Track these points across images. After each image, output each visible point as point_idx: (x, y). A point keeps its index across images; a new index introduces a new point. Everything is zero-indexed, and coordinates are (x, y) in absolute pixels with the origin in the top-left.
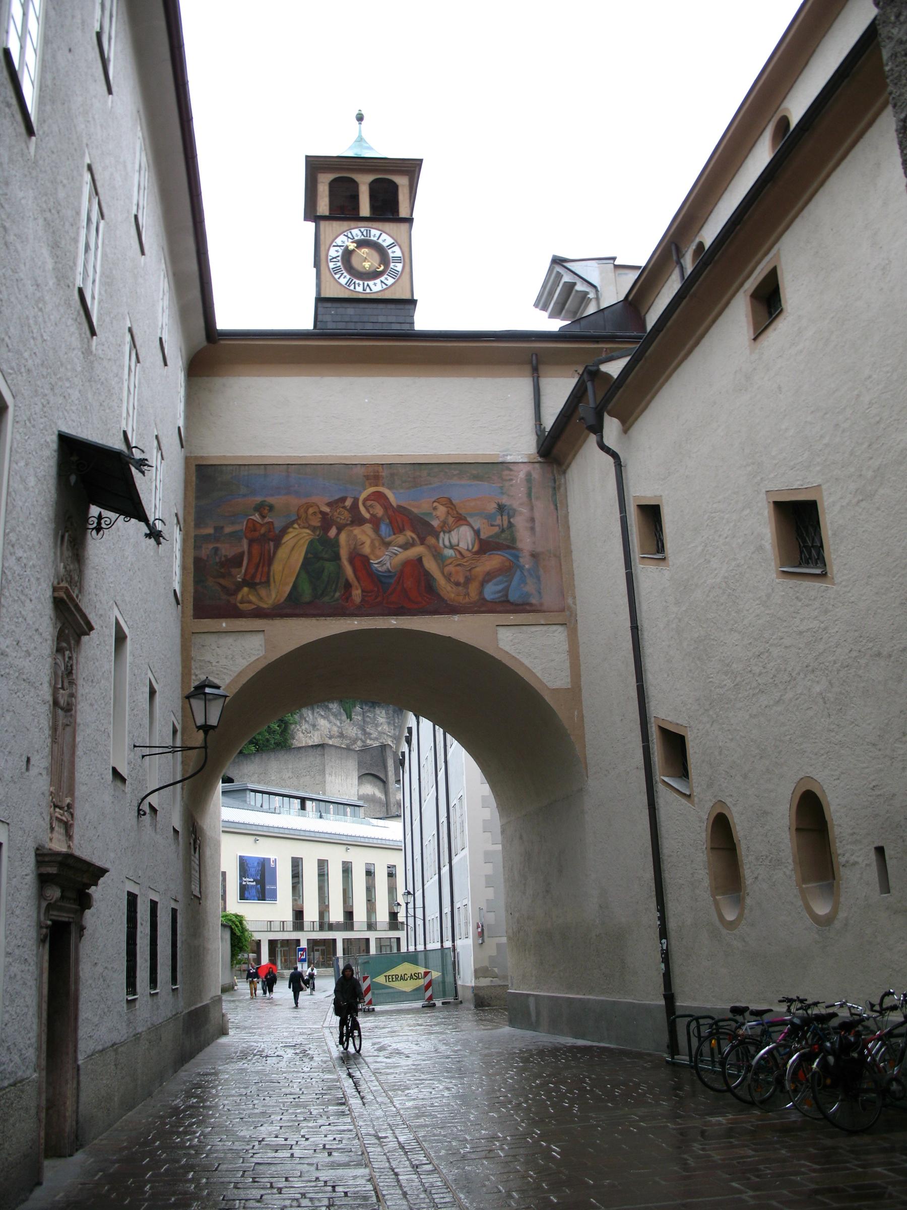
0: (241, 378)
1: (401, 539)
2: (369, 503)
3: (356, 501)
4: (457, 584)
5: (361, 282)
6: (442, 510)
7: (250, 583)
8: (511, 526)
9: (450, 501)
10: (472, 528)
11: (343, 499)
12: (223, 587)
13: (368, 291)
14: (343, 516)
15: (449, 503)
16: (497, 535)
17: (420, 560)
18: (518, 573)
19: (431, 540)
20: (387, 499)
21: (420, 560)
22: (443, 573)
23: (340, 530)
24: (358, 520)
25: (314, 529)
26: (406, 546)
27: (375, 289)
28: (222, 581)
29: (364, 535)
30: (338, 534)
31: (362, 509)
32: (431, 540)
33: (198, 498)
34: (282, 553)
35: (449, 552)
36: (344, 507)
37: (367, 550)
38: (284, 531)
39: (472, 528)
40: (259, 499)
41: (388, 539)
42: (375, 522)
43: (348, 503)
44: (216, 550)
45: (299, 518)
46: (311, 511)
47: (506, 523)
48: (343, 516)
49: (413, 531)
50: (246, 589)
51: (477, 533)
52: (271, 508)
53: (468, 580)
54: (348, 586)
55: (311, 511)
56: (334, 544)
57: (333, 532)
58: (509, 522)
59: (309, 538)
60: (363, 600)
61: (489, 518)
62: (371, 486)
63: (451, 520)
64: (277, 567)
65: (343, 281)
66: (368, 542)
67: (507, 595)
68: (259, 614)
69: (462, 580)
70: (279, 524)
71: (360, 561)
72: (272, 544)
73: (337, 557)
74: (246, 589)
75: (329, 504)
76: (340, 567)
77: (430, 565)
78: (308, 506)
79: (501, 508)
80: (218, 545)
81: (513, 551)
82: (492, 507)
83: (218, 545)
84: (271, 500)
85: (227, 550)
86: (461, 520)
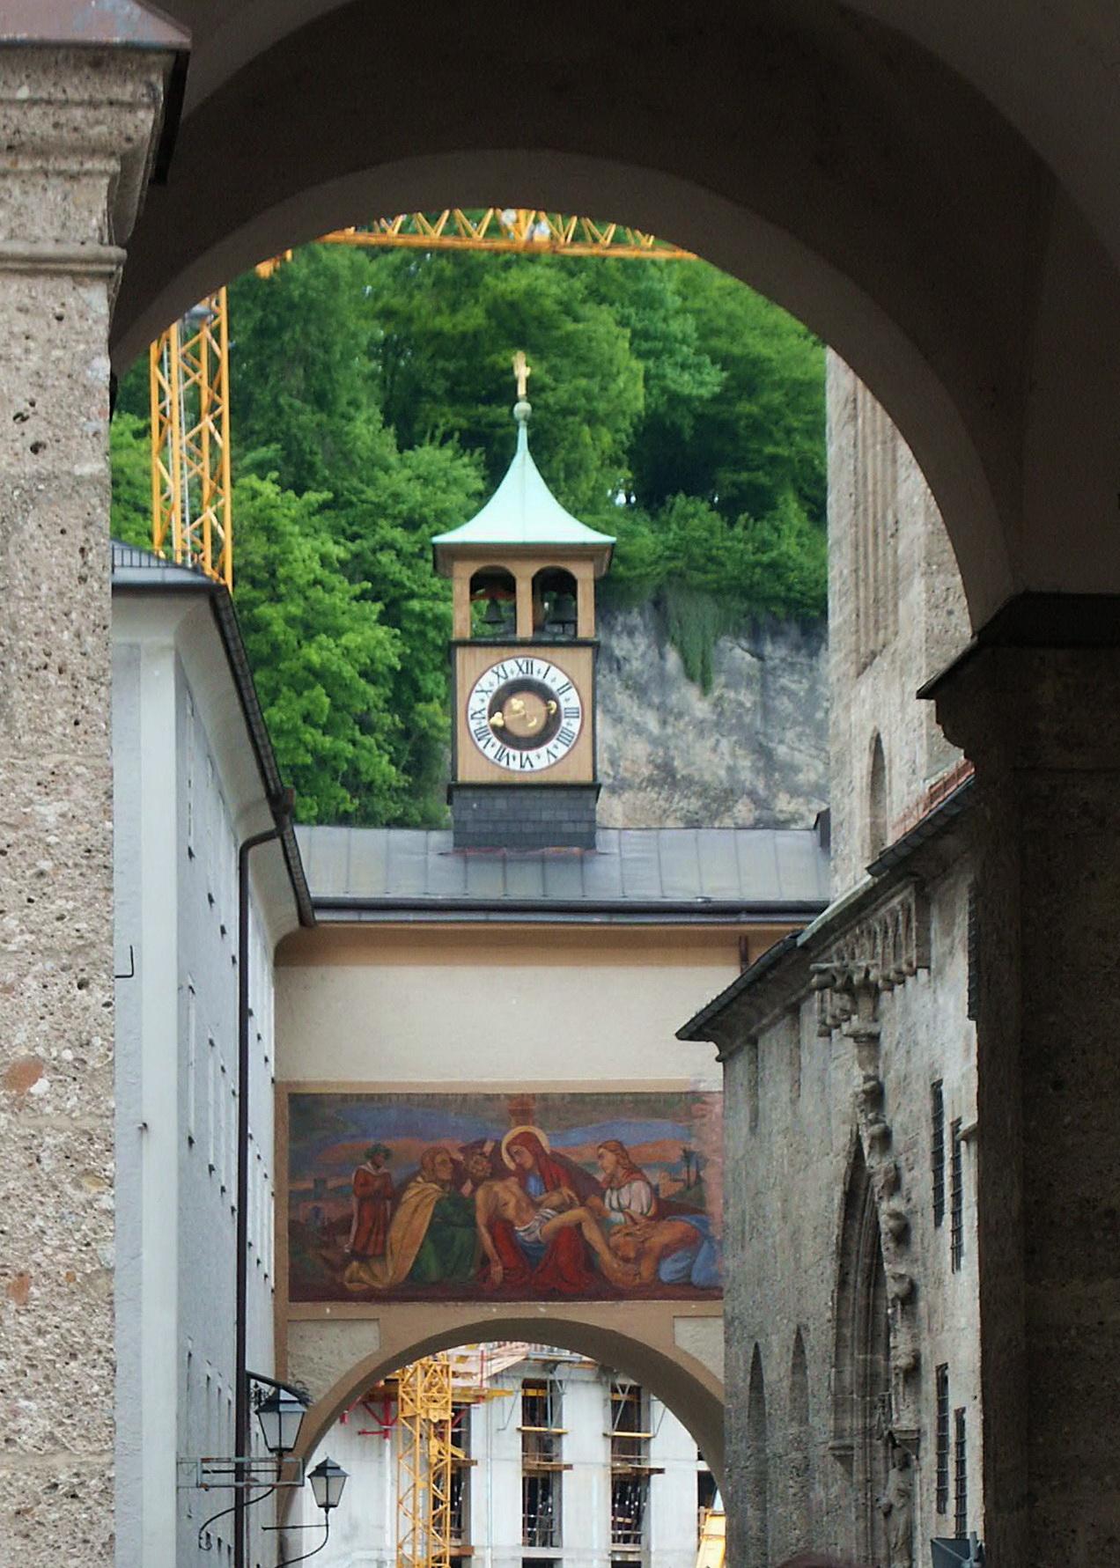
0: (348, 968)
1: (555, 1199)
2: (515, 1148)
3: (498, 1143)
4: (626, 1260)
5: (517, 753)
6: (610, 1158)
7: (361, 1256)
8: (699, 1180)
9: (620, 1144)
10: (649, 1183)
11: (482, 1143)
12: (326, 1261)
13: (528, 767)
14: (480, 1167)
15: (619, 1148)
16: (681, 1194)
17: (579, 1226)
18: (706, 1245)
19: (594, 1200)
20: (538, 1141)
21: (579, 1226)
22: (608, 1246)
23: (476, 1185)
24: (499, 1172)
25: (443, 1184)
26: (560, 1209)
27: (538, 765)
28: (324, 1252)
29: (507, 1193)
30: (473, 1191)
31: (505, 1156)
32: (594, 1200)
33: (293, 1139)
34: (402, 1215)
35: (618, 1217)
36: (482, 1154)
37: (510, 1212)
38: (404, 1187)
39: (649, 1183)
40: (372, 1141)
41: (539, 1199)
42: (522, 1174)
43: (488, 1148)
44: (317, 1211)
45: (424, 1168)
46: (439, 1159)
47: (693, 1178)
48: (480, 1167)
49: (571, 1188)
50: (355, 1264)
51: (655, 1190)
52: (388, 1154)
53: (638, 1259)
54: (486, 1261)
55: (439, 1159)
56: (467, 1206)
57: (467, 1188)
58: (698, 1176)
59: (435, 1196)
60: (505, 1280)
61: (671, 1170)
62: (518, 1124)
63: (621, 1172)
64: (395, 1233)
65: (490, 752)
66: (512, 1204)
67: (690, 1276)
68: (372, 1296)
69: (632, 1255)
70: (397, 1176)
71: (502, 1228)
72: (388, 1203)
73: (471, 1223)
74: (355, 1264)
75: (462, 1150)
76: (476, 1235)
77: (592, 1234)
78: (437, 1151)
79: (688, 1156)
80: (320, 1205)
81: (699, 1216)
82: (675, 1155)
83: (320, 1205)
84: (387, 1143)
85: (332, 1212)
86: (634, 1172)
